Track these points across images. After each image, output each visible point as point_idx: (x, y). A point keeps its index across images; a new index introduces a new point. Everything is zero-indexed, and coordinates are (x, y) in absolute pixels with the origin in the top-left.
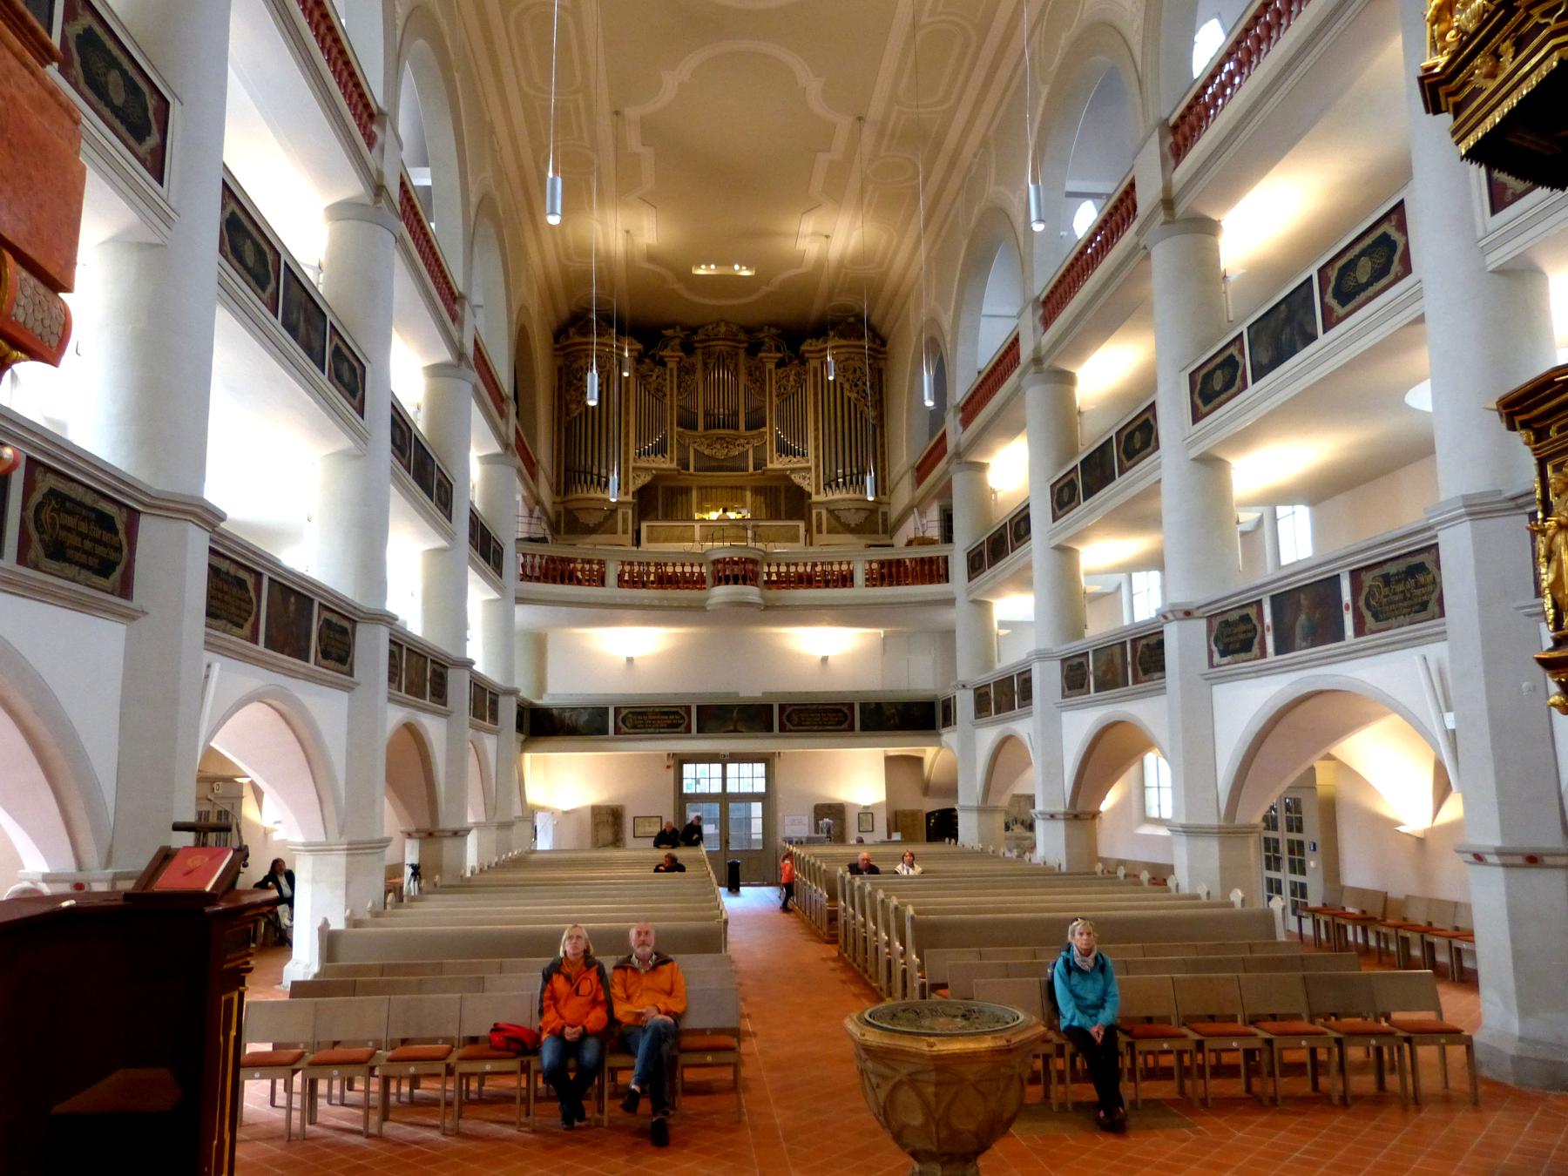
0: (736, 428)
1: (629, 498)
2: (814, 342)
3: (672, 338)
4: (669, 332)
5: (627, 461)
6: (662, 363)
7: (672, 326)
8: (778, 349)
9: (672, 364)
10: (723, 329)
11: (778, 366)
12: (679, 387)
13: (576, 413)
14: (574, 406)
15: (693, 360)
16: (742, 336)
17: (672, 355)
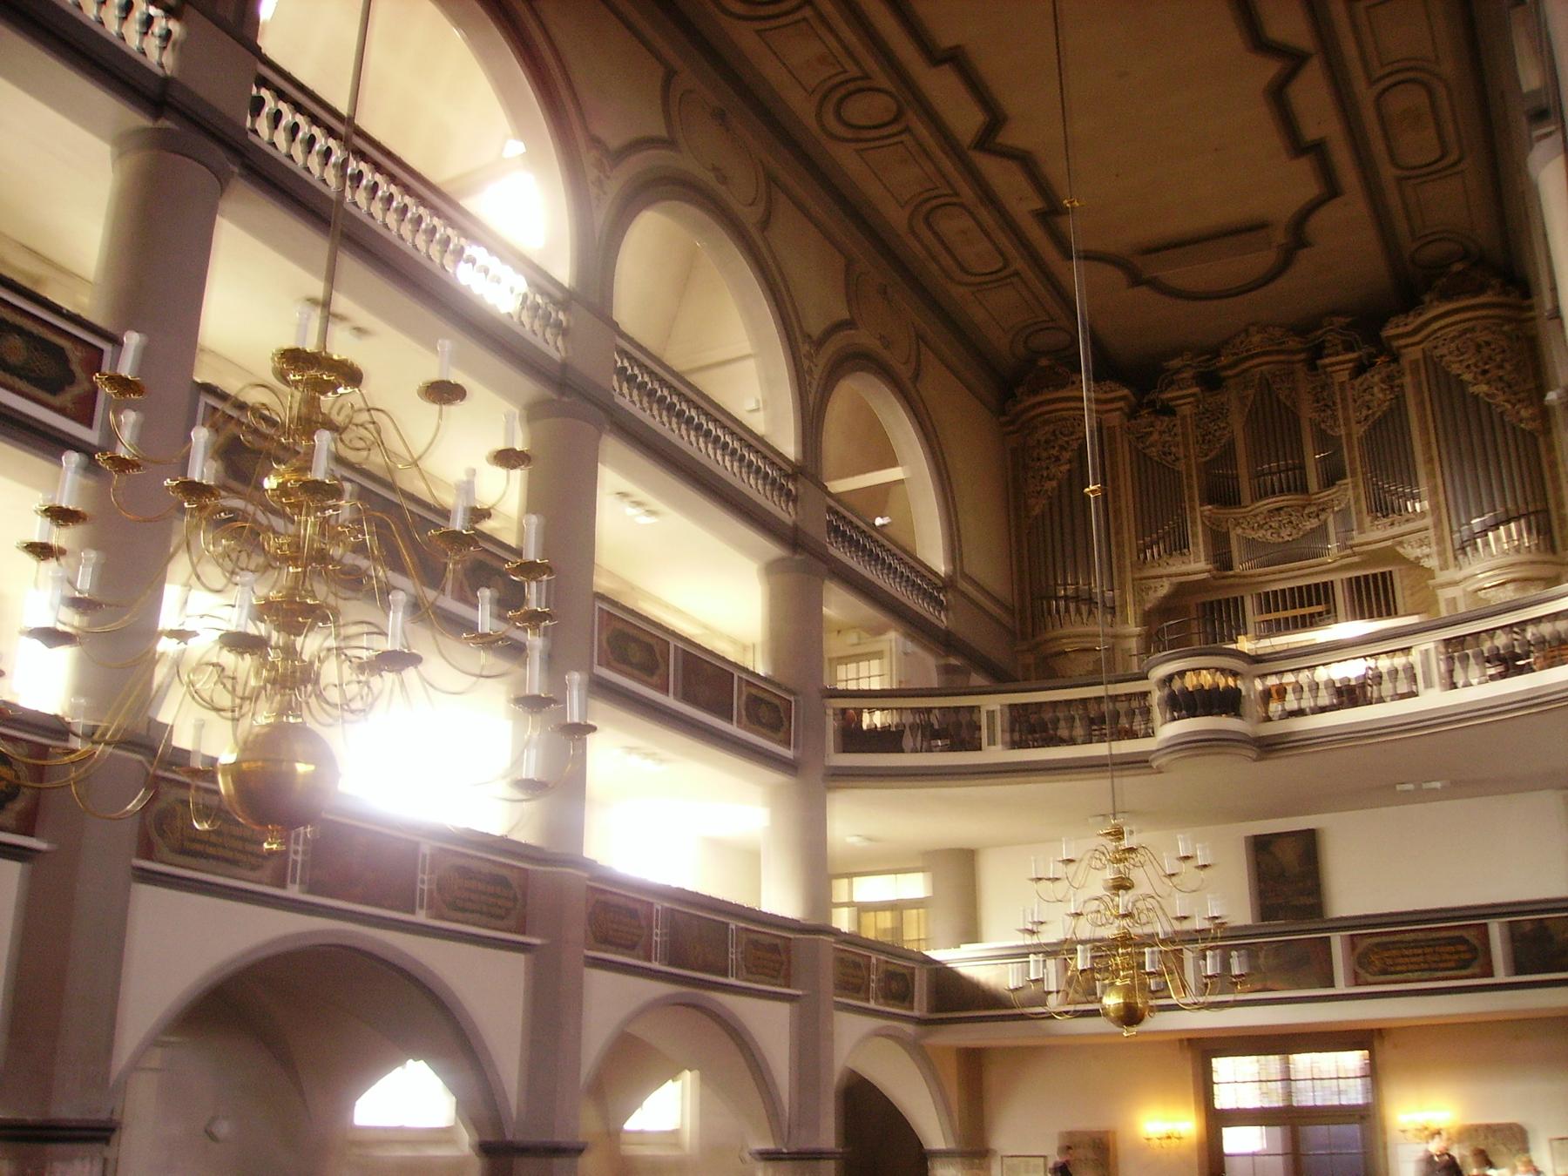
2: (1401, 319)
4: (1176, 363)
6: (1168, 410)
7: (1177, 352)
8: (1349, 348)
9: (1186, 410)
13: (1037, 511)
14: (1032, 501)
17: (1184, 396)
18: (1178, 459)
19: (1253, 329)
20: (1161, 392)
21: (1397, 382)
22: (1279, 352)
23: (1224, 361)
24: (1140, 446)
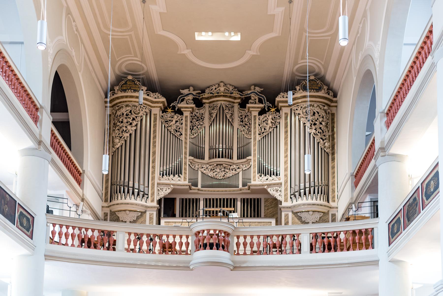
0: (231, 158)
1: (155, 204)
3: (187, 95)
4: (186, 92)
5: (153, 178)
8: (260, 101)
9: (187, 114)
10: (222, 89)
11: (260, 113)
12: (192, 129)
15: (202, 111)
16: (236, 94)
18: (181, 134)
19: (222, 84)
20: (178, 103)
21: (278, 121)
22: (230, 97)
23: (206, 95)
24: (167, 125)
